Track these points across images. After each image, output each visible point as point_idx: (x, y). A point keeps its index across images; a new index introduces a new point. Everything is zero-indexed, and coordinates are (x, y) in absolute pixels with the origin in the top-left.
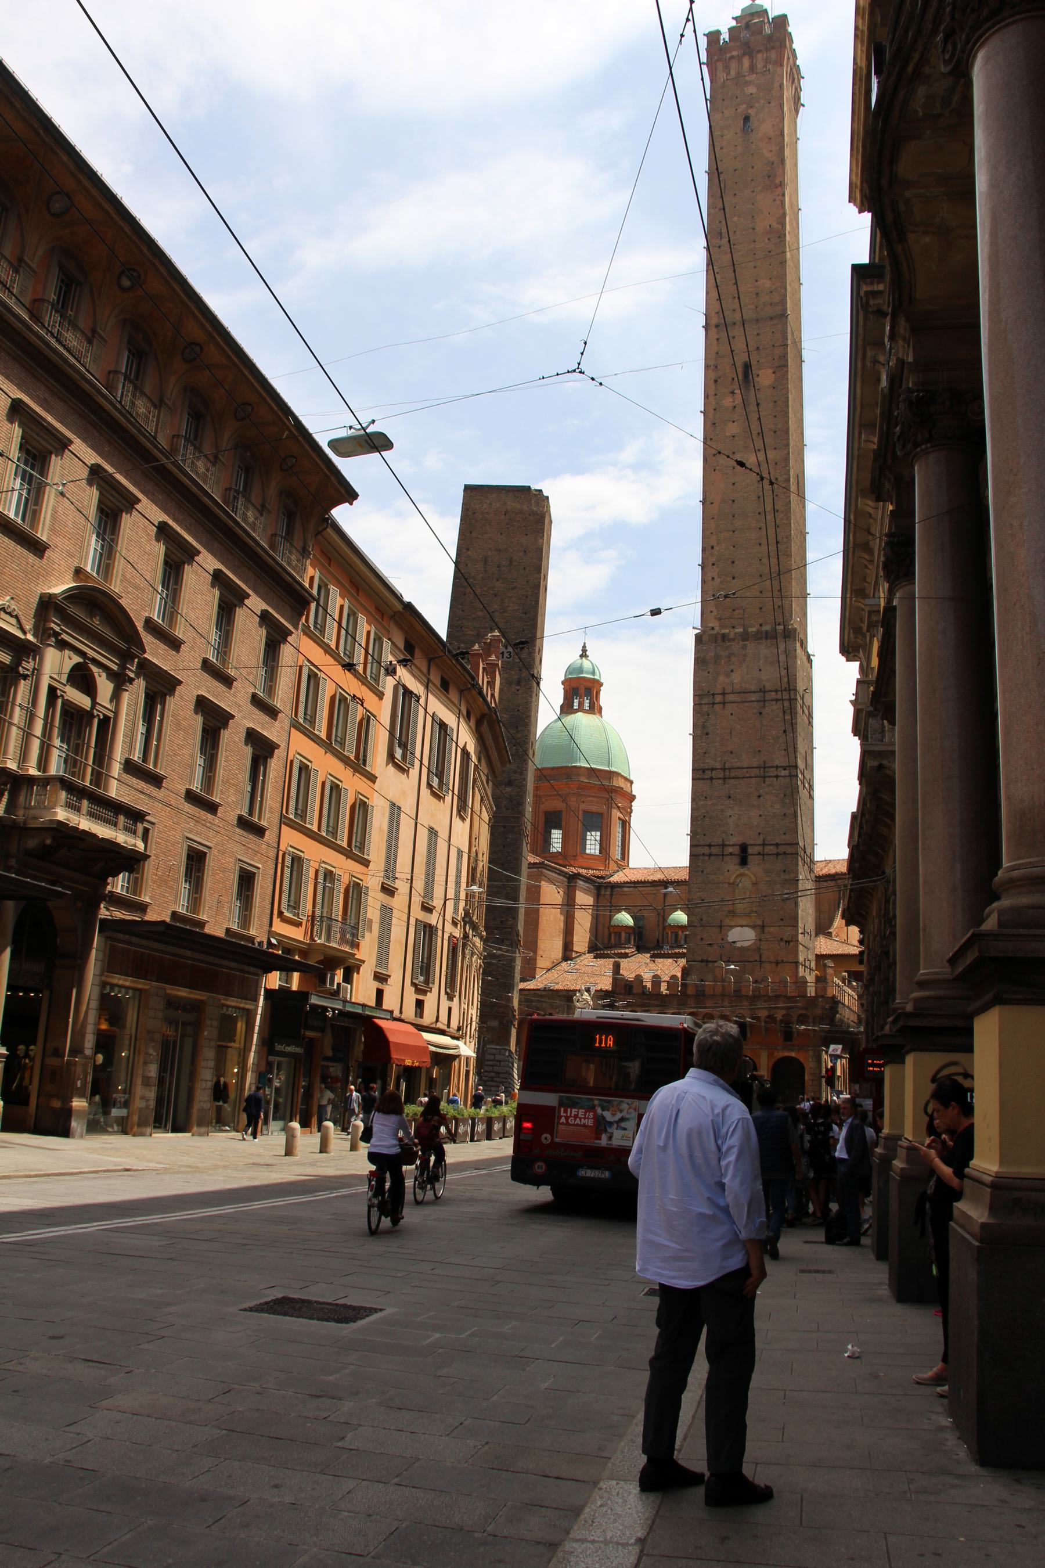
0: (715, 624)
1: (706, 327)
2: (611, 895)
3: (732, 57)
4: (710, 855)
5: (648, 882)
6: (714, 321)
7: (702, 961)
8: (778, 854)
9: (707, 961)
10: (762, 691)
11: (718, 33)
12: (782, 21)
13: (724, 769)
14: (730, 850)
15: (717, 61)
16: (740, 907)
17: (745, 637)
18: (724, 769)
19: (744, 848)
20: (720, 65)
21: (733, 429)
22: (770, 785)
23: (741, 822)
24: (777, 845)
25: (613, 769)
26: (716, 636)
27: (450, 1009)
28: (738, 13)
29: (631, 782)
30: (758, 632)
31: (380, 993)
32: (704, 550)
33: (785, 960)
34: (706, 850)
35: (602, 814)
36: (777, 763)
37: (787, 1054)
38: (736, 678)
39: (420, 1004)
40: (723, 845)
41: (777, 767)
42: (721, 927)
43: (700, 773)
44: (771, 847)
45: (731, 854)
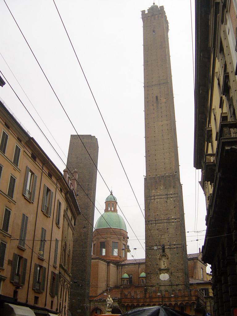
1: (144, 87)
2: (122, 268)
3: (149, 16)
5: (133, 264)
11: (144, 11)
12: (162, 8)
13: (155, 221)
22: (171, 225)
27: (52, 302)
29: (127, 233)
31: (15, 293)
32: (146, 152)
33: (179, 284)
35: (118, 242)
39: (36, 298)
44: (172, 246)
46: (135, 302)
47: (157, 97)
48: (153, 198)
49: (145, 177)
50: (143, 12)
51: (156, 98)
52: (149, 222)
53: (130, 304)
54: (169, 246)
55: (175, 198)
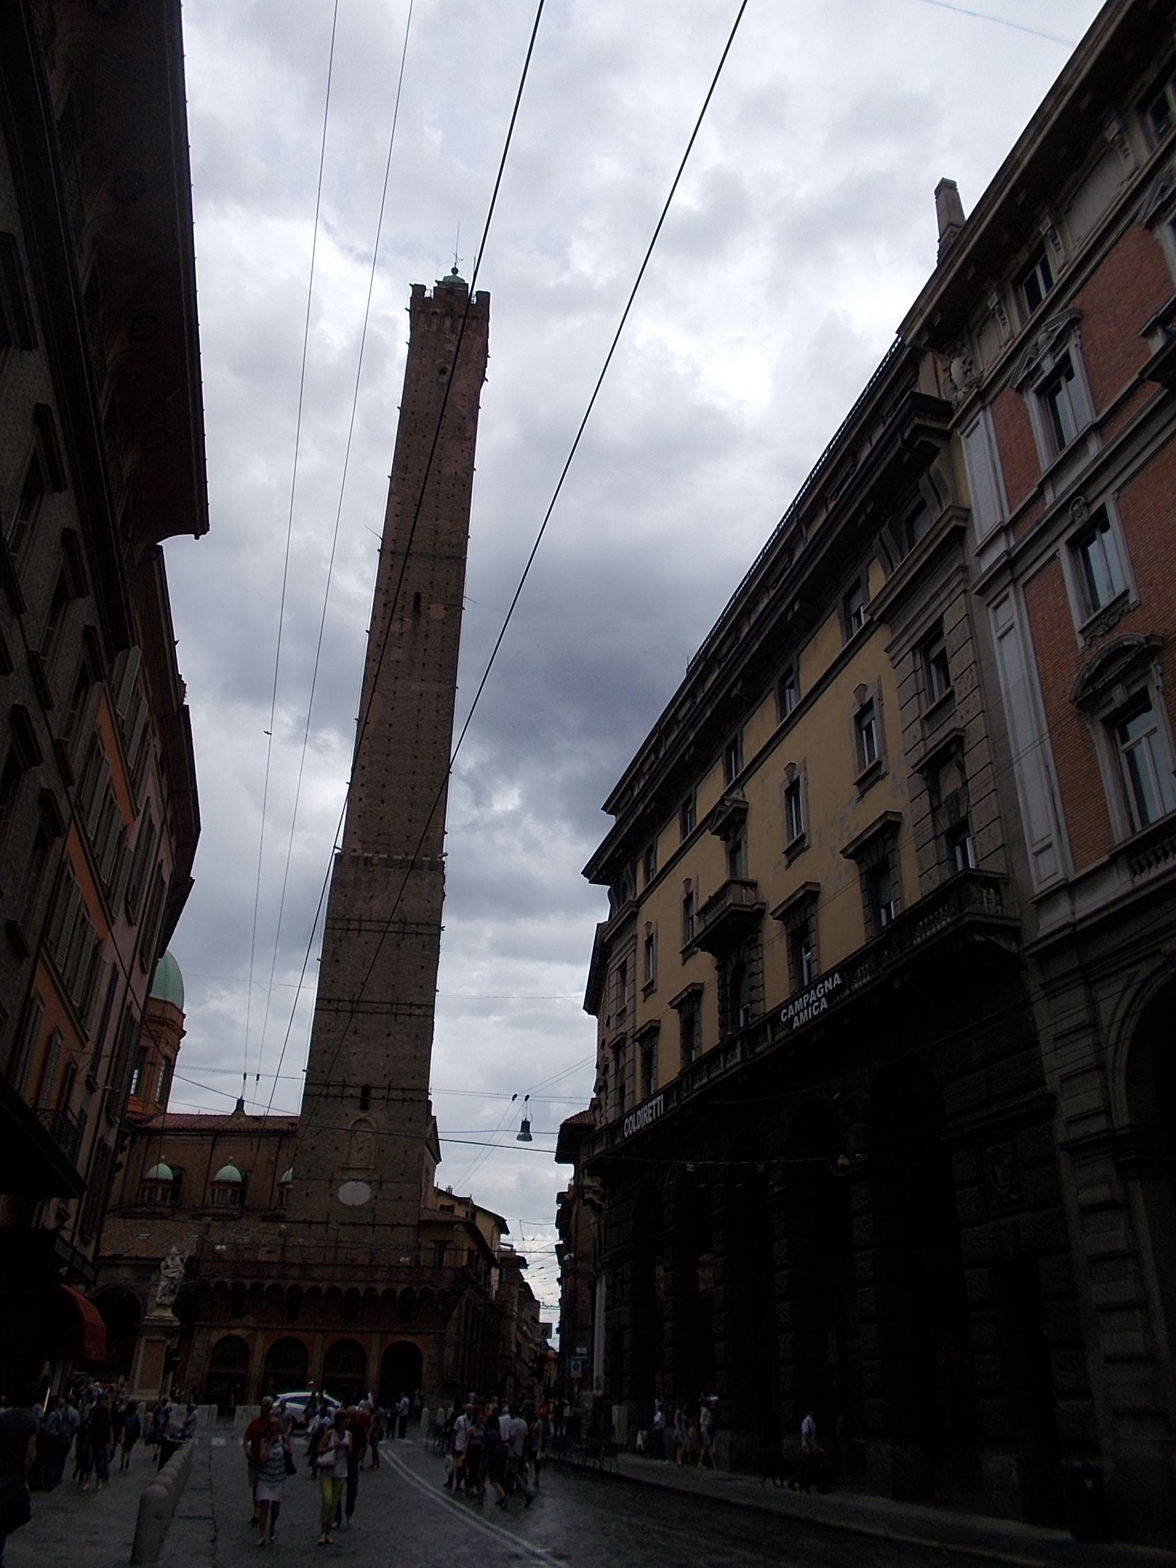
0: (358, 846)
2: (148, 1144)
3: (434, 313)
4: (327, 1096)
5: (195, 1130)
6: (391, 547)
7: (304, 1222)
8: (404, 1100)
9: (311, 1223)
10: (404, 922)
11: (424, 288)
12: (484, 297)
13: (352, 1002)
14: (351, 1091)
15: (423, 312)
17: (389, 863)
18: (352, 1002)
19: (366, 1090)
24: (404, 1090)
25: (169, 1000)
26: (358, 857)
28: (441, 279)
30: (402, 861)
36: (411, 1000)
41: (411, 1005)
42: (331, 1181)
45: (351, 1096)
46: (245, 1276)
47: (418, 597)
49: (337, 851)
50: (418, 290)
51: (412, 599)
52: (329, 1001)
54: (385, 1092)
55: (427, 939)
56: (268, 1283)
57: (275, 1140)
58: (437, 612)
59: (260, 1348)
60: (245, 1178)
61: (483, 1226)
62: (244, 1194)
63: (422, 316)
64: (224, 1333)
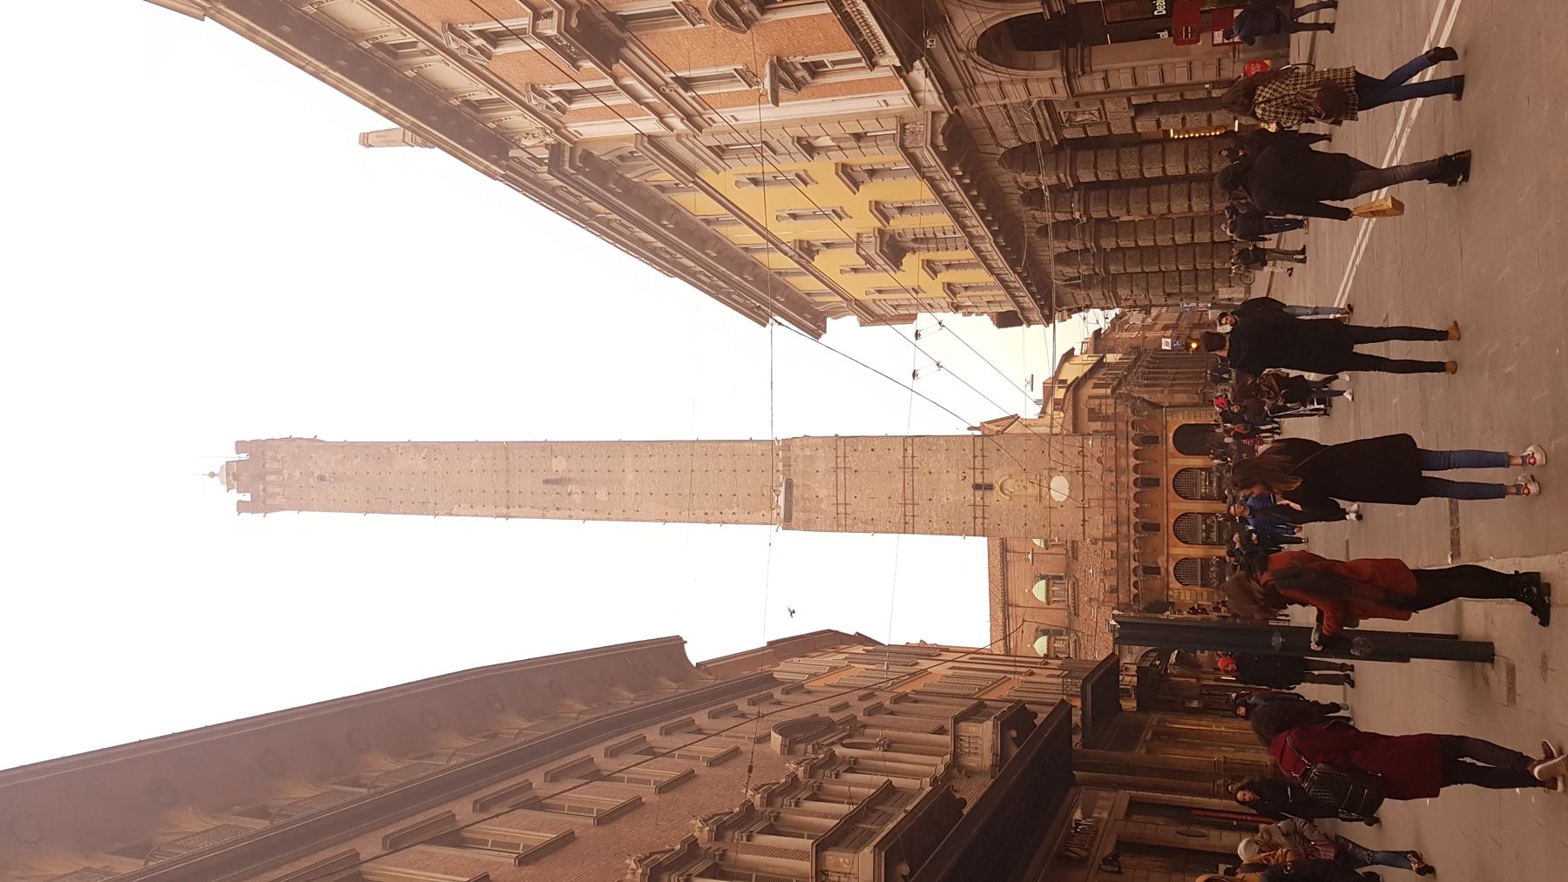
1: (507, 517)
6: (504, 510)
11: (239, 502)
16: (1033, 490)
19: (977, 487)
20: (269, 502)
21: (602, 495)
23: (954, 491)
32: (708, 522)
34: (979, 521)
36: (900, 457)
37: (1171, 441)
38: (823, 493)
40: (974, 505)
43: (907, 526)
47: (546, 482)
48: (841, 509)
50: (242, 507)
53: (1133, 579)
56: (1133, 550)
57: (1009, 556)
58: (559, 465)
59: (1181, 551)
60: (1042, 577)
61: (1071, 373)
62: (1054, 577)
63: (269, 502)
64: (1172, 578)
